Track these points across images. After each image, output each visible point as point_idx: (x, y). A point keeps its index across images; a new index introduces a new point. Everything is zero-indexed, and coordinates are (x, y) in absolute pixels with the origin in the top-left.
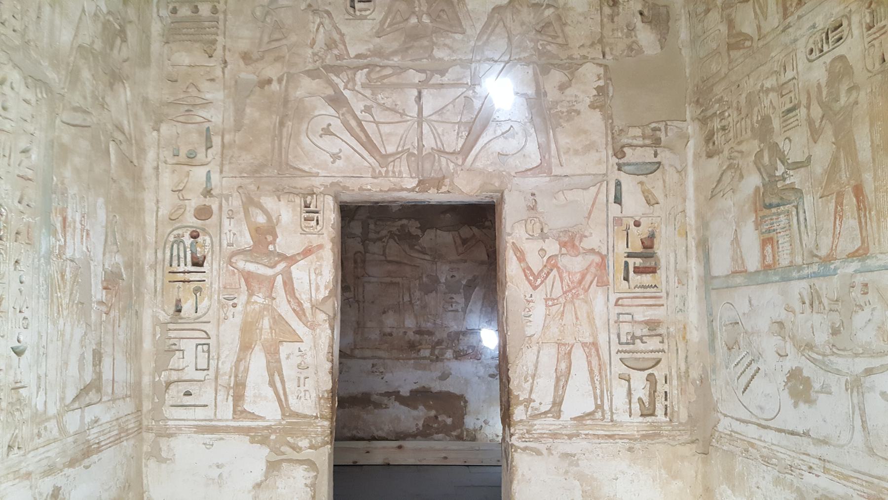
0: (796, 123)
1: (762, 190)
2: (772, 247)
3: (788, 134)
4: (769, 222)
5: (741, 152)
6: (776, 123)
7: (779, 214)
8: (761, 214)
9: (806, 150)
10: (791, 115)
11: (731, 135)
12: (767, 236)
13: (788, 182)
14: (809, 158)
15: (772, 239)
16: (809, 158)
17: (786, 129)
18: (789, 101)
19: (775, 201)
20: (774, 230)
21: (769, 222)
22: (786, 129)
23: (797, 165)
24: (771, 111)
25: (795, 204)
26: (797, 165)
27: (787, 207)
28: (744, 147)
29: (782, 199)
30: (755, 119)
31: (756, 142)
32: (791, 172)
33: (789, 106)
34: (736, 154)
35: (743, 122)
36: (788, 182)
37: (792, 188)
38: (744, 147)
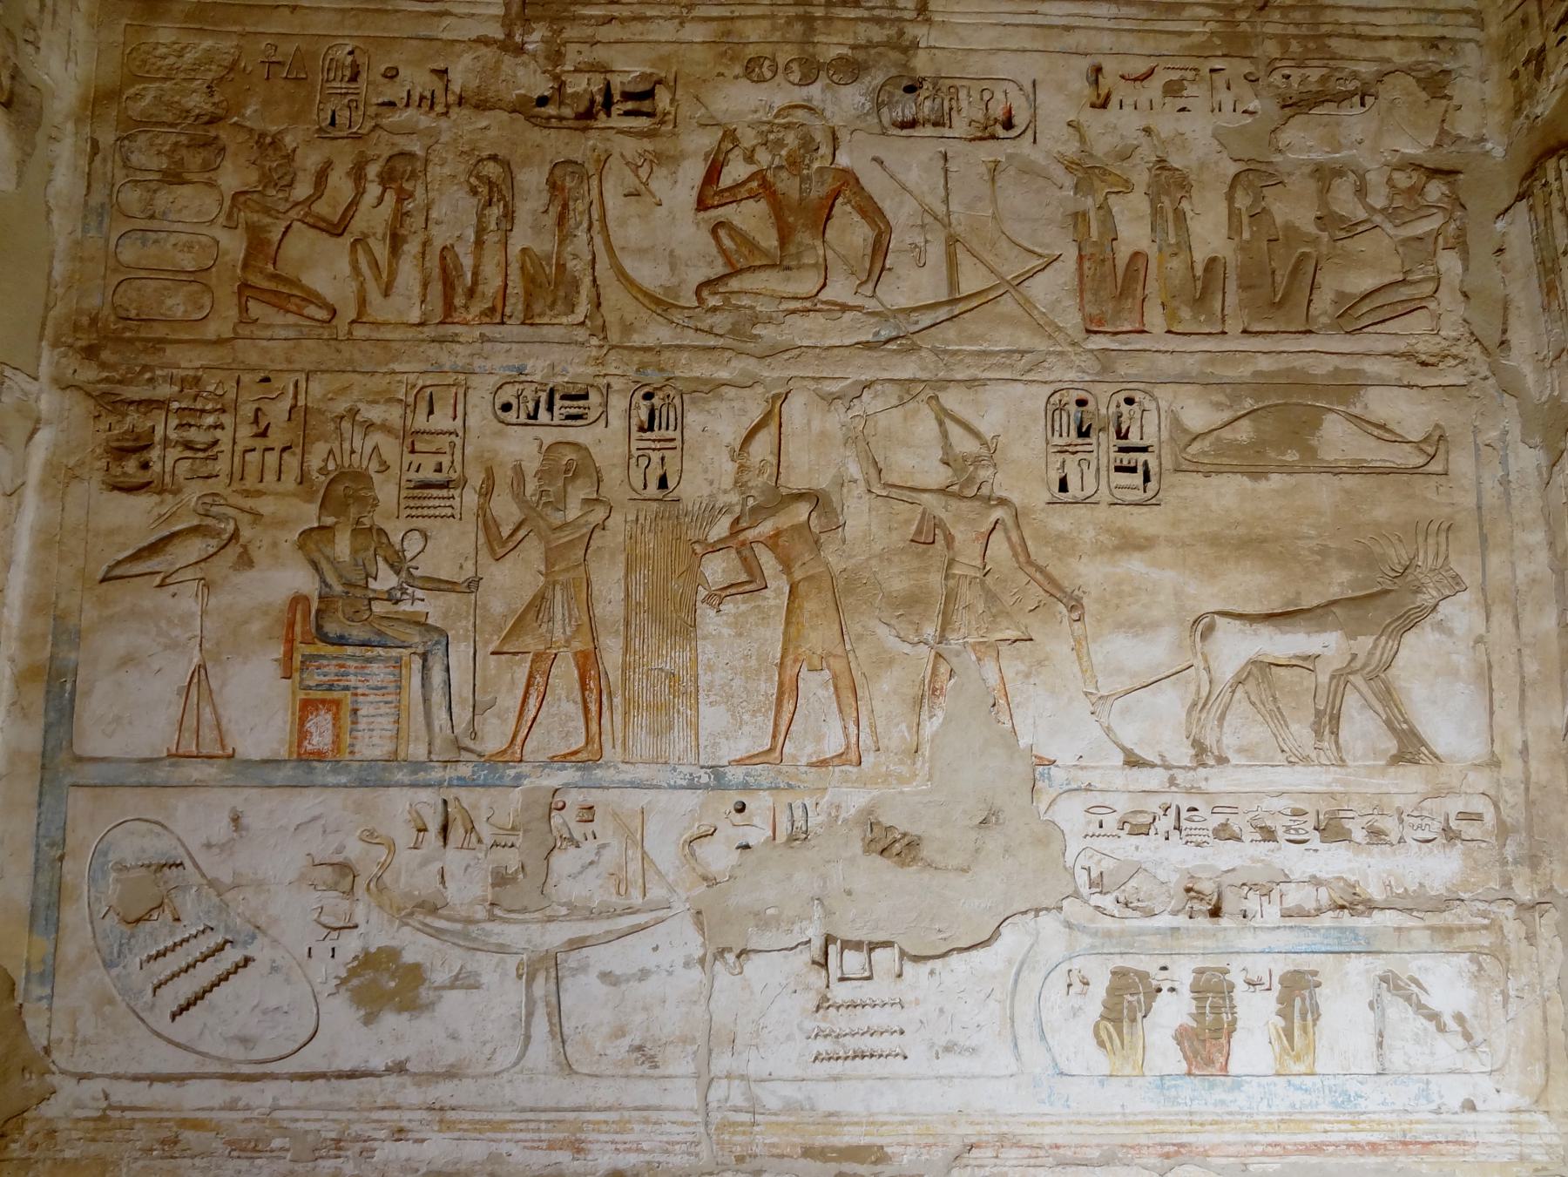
0: (449, 511)
1: (315, 606)
2: (336, 718)
3: (420, 523)
4: (333, 669)
5: (257, 516)
6: (386, 492)
7: (370, 660)
8: (303, 649)
9: (469, 566)
10: (435, 492)
11: (222, 466)
12: (318, 695)
13: (405, 607)
14: (473, 584)
15: (337, 703)
16: (473, 584)
17: (414, 512)
18: (433, 466)
19: (358, 633)
20: (346, 688)
21: (333, 669)
22: (414, 512)
23: (436, 585)
24: (374, 466)
25: (421, 650)
26: (436, 585)
27: (395, 653)
28: (266, 506)
29: (380, 633)
30: (315, 462)
31: (312, 509)
32: (419, 594)
33: (428, 474)
34: (231, 512)
35: (271, 458)
36: (405, 607)
37: (420, 623)
38: (266, 506)
